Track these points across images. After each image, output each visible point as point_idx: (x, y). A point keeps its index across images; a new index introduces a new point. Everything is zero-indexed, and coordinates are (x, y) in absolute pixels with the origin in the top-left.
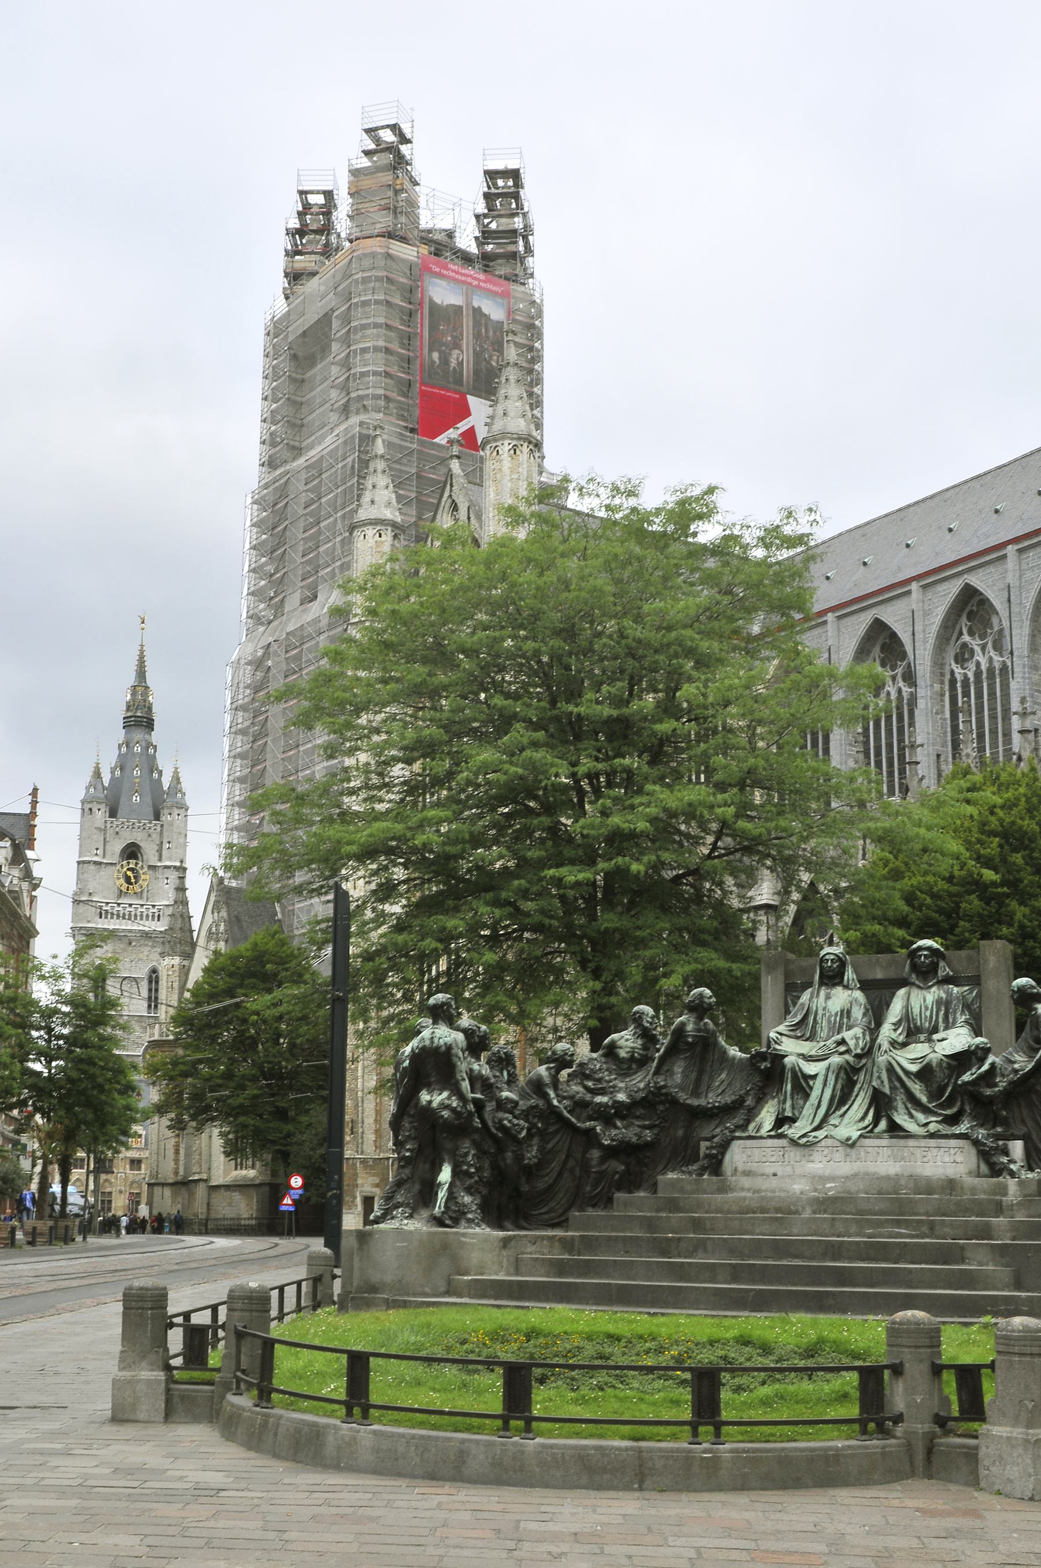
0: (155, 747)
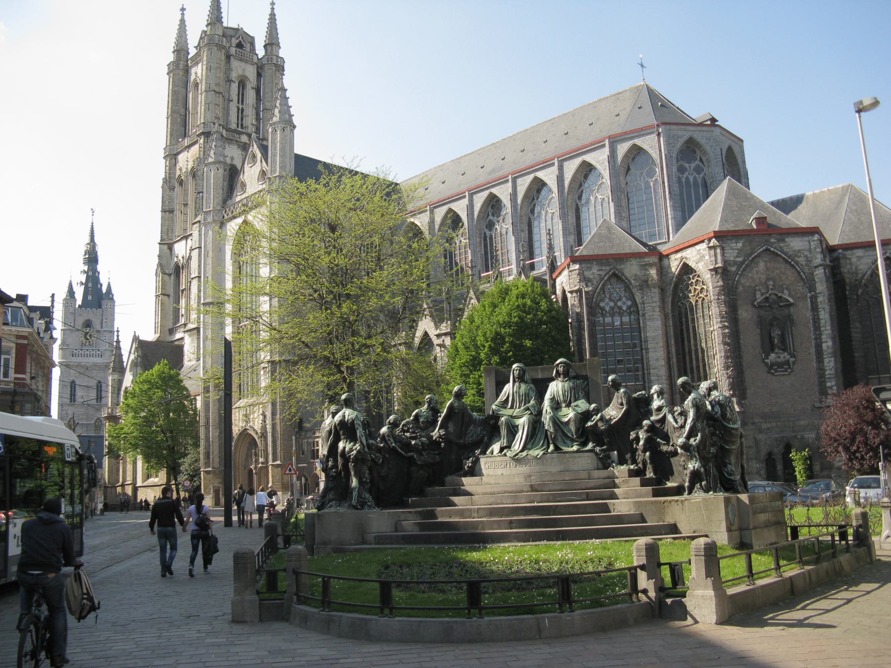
0: (99, 273)
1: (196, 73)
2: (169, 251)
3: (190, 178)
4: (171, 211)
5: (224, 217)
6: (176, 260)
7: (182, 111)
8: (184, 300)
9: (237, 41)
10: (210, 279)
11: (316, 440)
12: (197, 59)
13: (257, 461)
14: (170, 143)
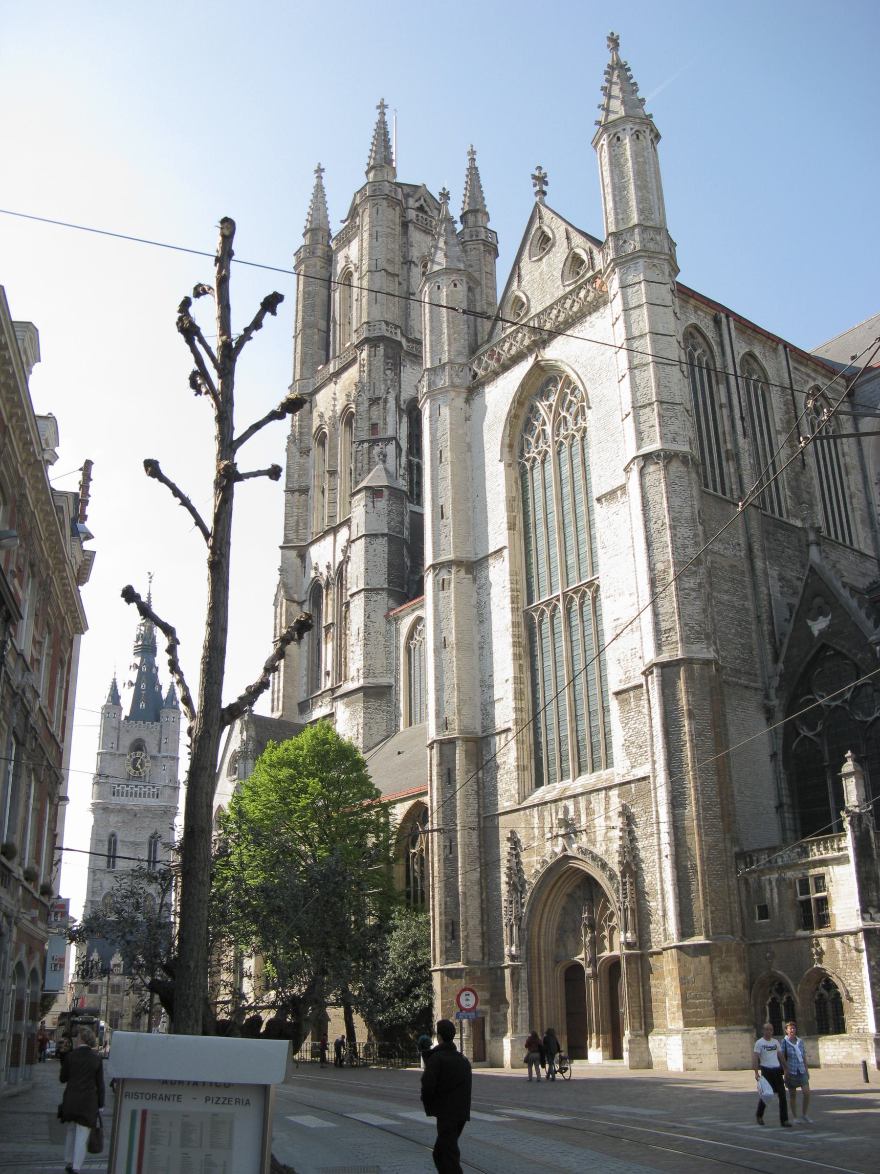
0: (157, 669)
1: (347, 257)
2: (298, 561)
3: (341, 427)
4: (304, 491)
5: (475, 375)
6: (313, 574)
7: (322, 324)
8: (330, 645)
9: (417, 205)
10: (449, 511)
11: (813, 872)
12: (345, 239)
13: (597, 945)
14: (301, 375)
